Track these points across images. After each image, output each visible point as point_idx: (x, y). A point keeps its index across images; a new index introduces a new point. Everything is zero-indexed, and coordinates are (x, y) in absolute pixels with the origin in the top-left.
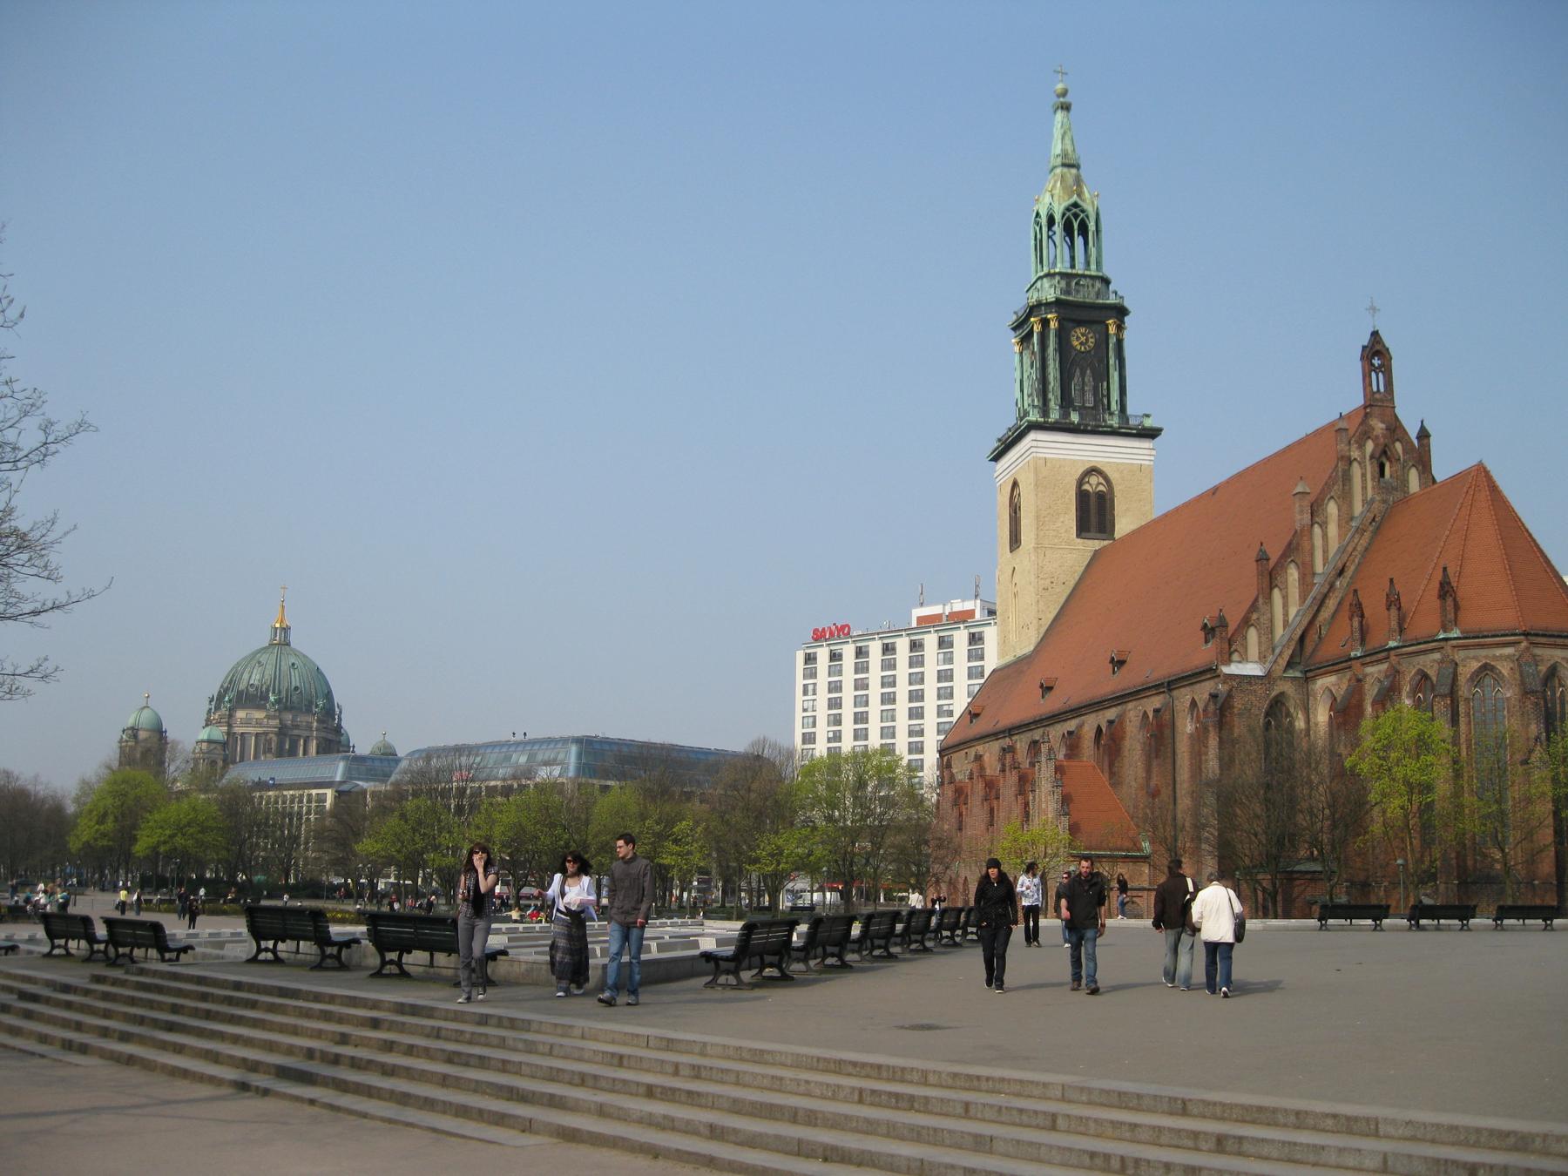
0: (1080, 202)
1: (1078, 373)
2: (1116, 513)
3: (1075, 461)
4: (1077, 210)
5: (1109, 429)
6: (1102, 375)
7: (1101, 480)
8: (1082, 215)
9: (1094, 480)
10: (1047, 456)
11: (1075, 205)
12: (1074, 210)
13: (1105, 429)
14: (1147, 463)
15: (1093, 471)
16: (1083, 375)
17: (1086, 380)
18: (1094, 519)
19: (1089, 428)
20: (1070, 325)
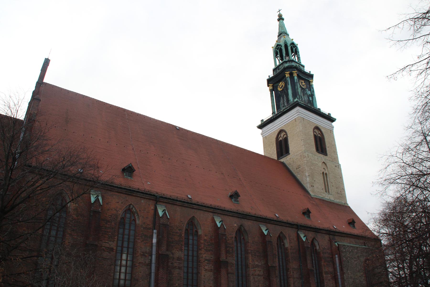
0: (278, 43)
1: (282, 98)
2: (289, 143)
3: (274, 132)
4: (278, 47)
5: (281, 113)
6: (287, 95)
7: (285, 133)
8: (279, 47)
9: (282, 135)
10: (266, 135)
11: (278, 45)
12: (277, 47)
13: (279, 114)
14: (297, 116)
15: (281, 131)
16: (283, 98)
17: (284, 99)
18: (284, 149)
19: (274, 117)
20: (277, 84)
